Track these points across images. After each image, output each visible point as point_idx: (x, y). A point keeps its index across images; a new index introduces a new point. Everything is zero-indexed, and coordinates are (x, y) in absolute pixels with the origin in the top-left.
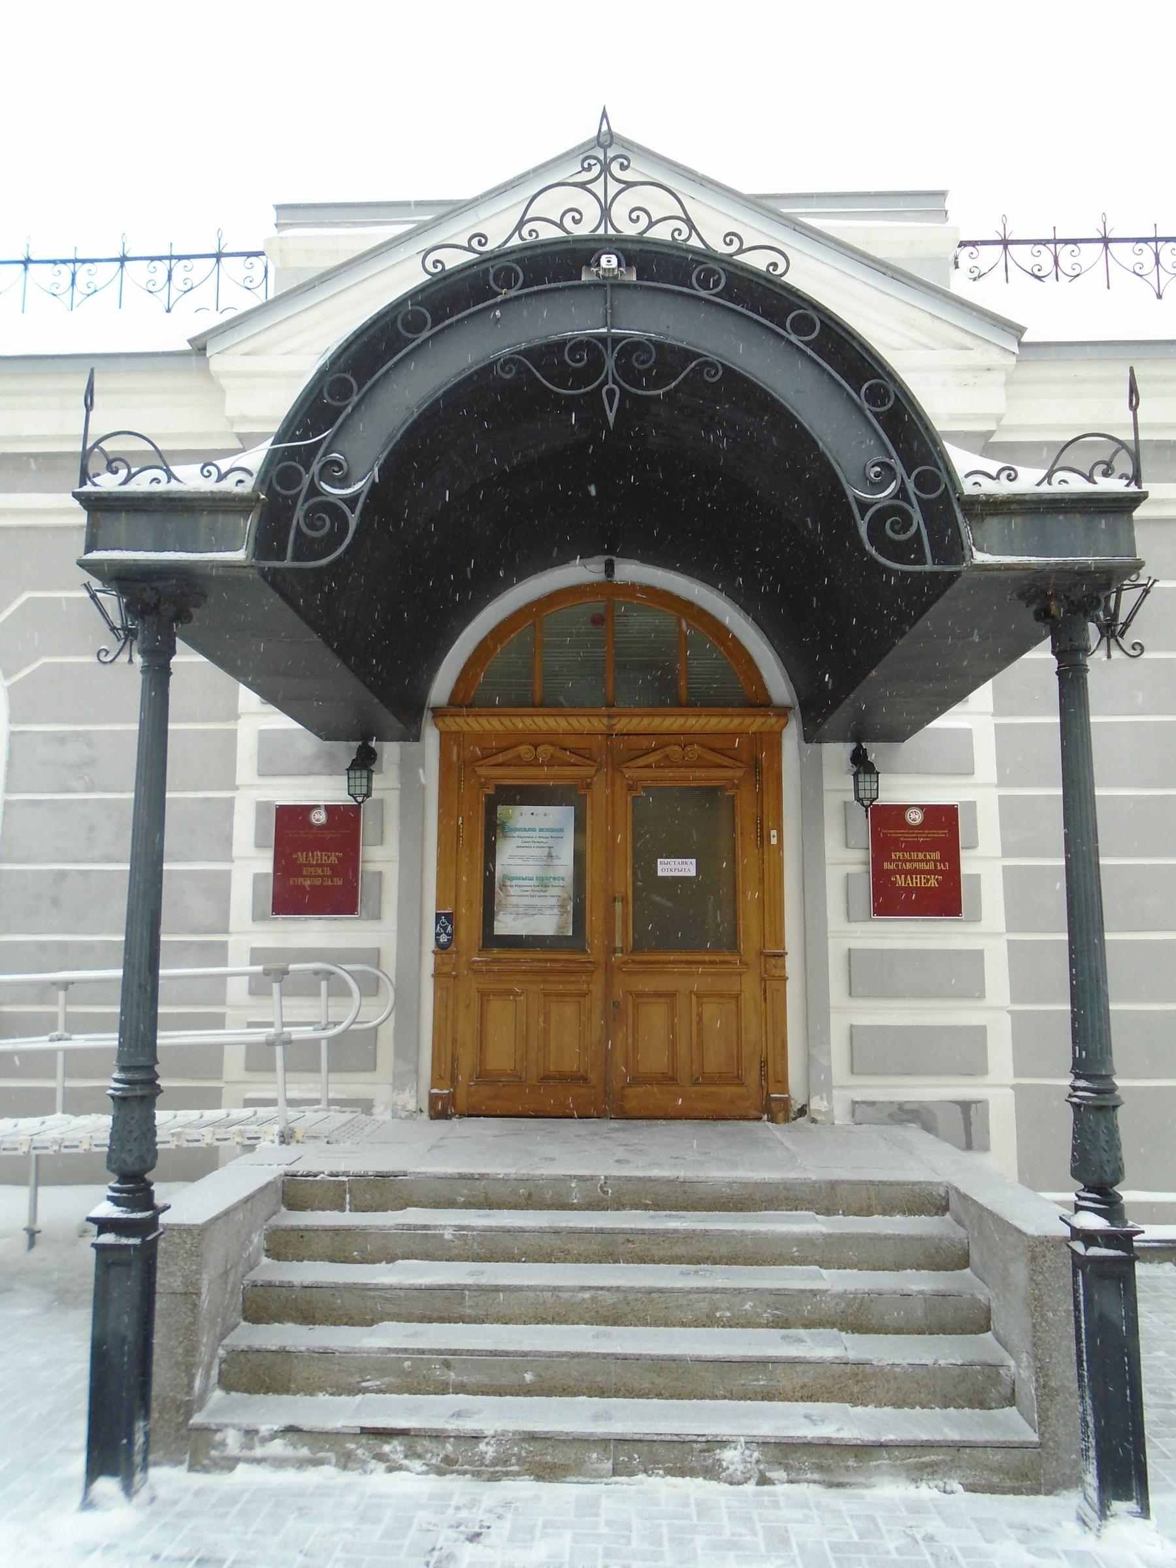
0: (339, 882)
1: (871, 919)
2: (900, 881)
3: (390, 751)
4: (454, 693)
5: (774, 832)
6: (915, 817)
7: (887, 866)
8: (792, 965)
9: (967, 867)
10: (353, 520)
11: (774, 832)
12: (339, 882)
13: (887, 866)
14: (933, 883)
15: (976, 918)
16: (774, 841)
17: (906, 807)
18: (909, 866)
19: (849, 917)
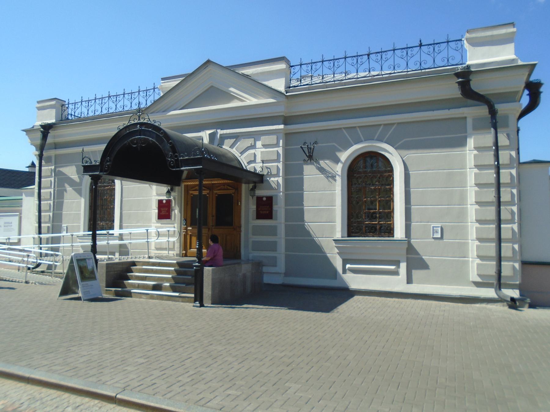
0: (167, 213)
1: (255, 220)
2: (261, 212)
3: (177, 188)
4: (187, 176)
5: (239, 202)
6: (265, 199)
7: (259, 209)
8: (243, 229)
9: (275, 208)
10: (110, 166)
11: (239, 202)
12: (167, 213)
13: (259, 209)
14: (267, 212)
15: (276, 220)
16: (239, 204)
17: (263, 197)
18: (263, 209)
19: (253, 220)
